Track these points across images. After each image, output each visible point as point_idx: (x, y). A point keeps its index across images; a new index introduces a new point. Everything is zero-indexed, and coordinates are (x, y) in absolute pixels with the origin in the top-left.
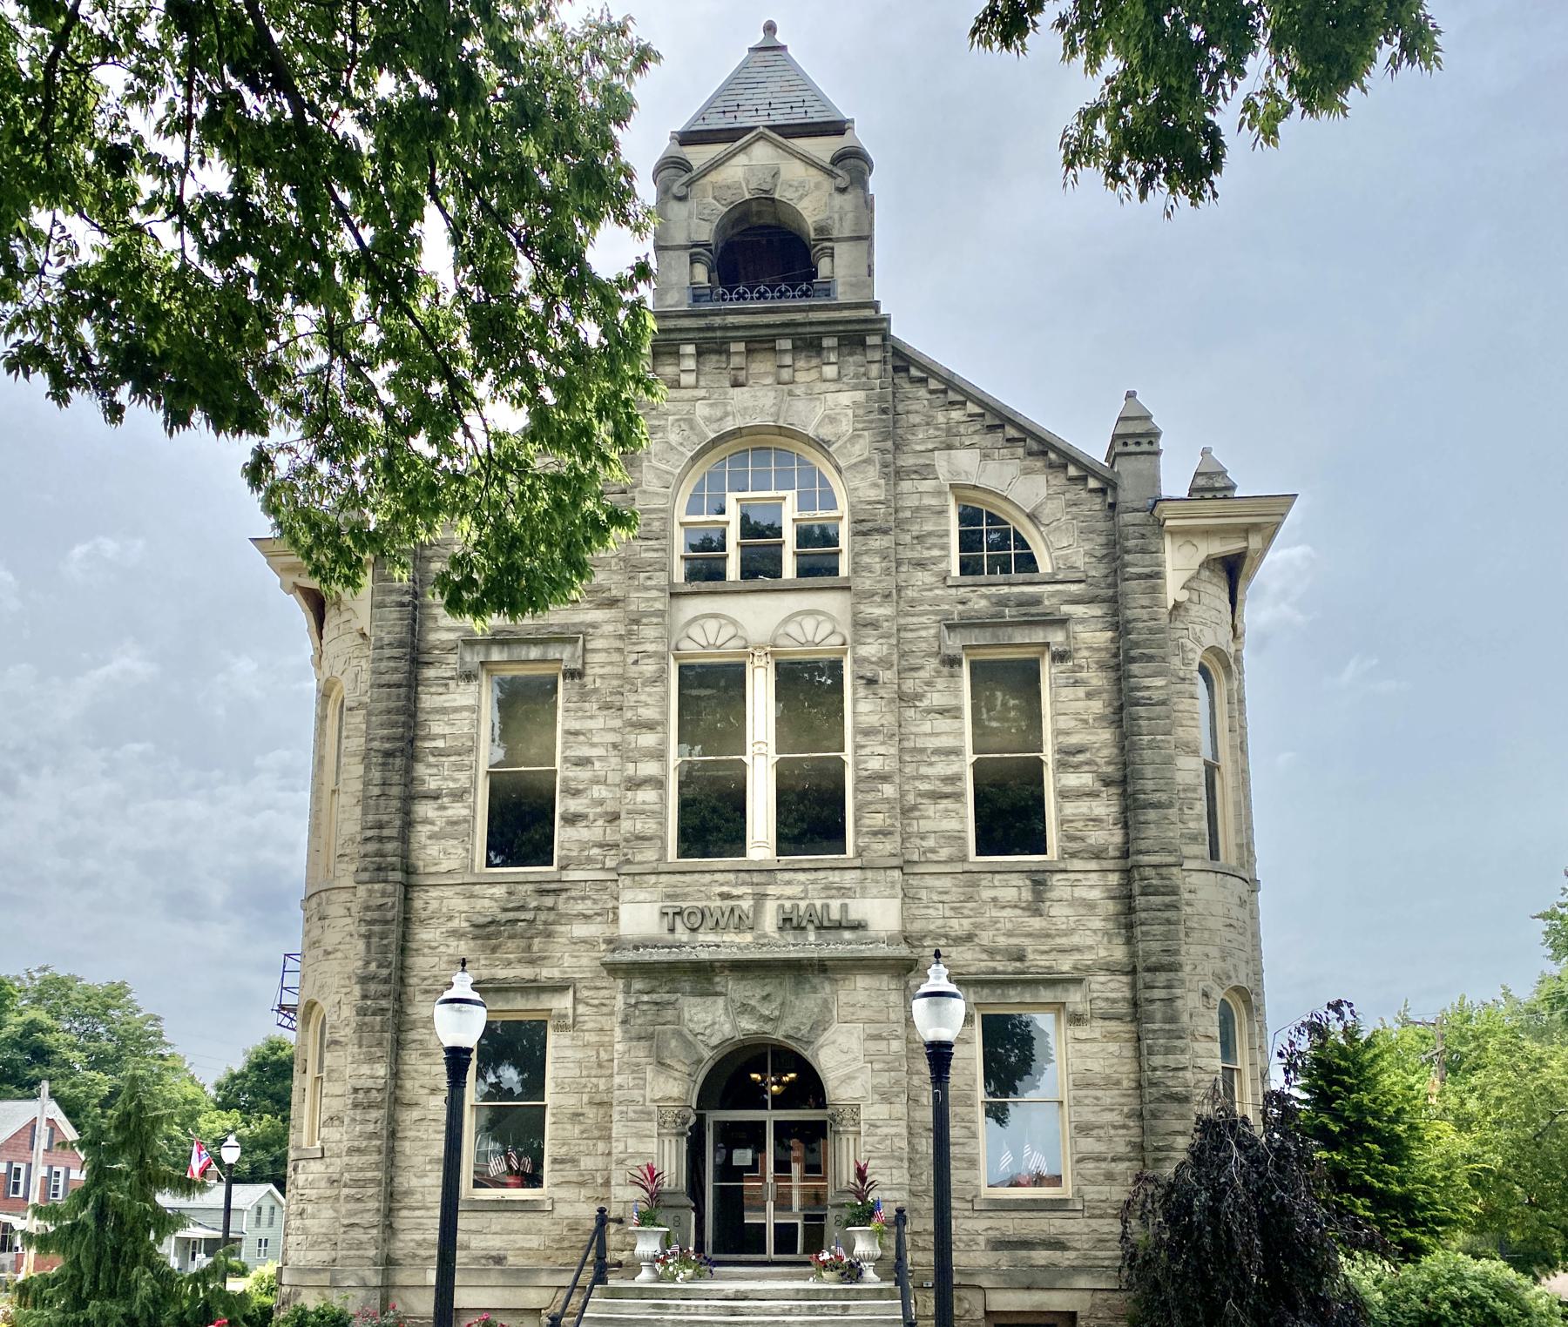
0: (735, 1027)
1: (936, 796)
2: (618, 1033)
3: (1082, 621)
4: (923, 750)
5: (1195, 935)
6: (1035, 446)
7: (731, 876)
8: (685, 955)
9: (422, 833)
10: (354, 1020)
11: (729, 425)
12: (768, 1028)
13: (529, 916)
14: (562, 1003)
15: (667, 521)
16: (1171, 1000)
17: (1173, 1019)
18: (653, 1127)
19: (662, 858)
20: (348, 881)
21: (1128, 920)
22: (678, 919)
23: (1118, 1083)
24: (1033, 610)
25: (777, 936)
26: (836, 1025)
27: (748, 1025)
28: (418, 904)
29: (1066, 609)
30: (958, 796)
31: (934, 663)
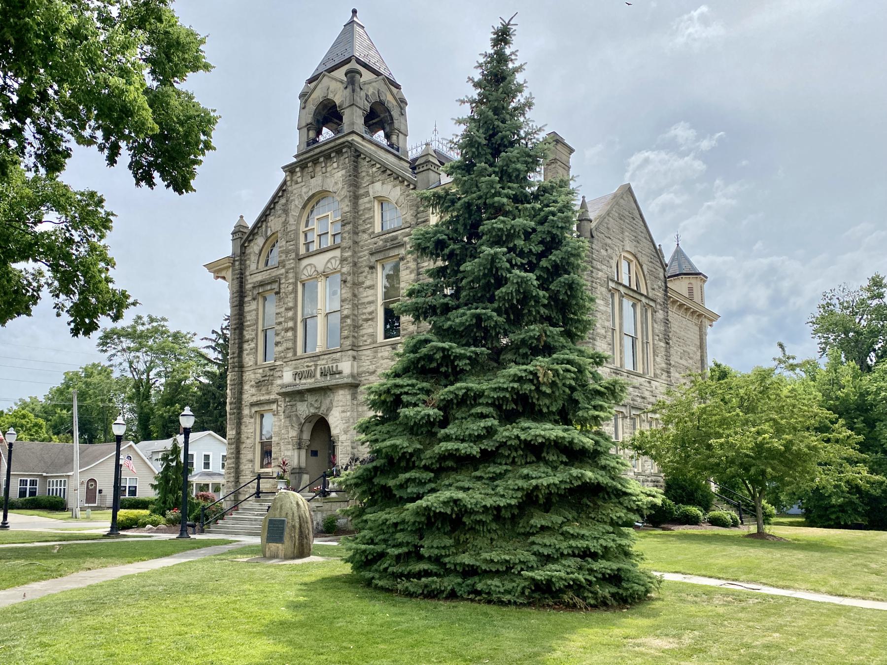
1: (367, 320)
4: (363, 303)
9: (245, 352)
19: (295, 354)
27: (313, 411)
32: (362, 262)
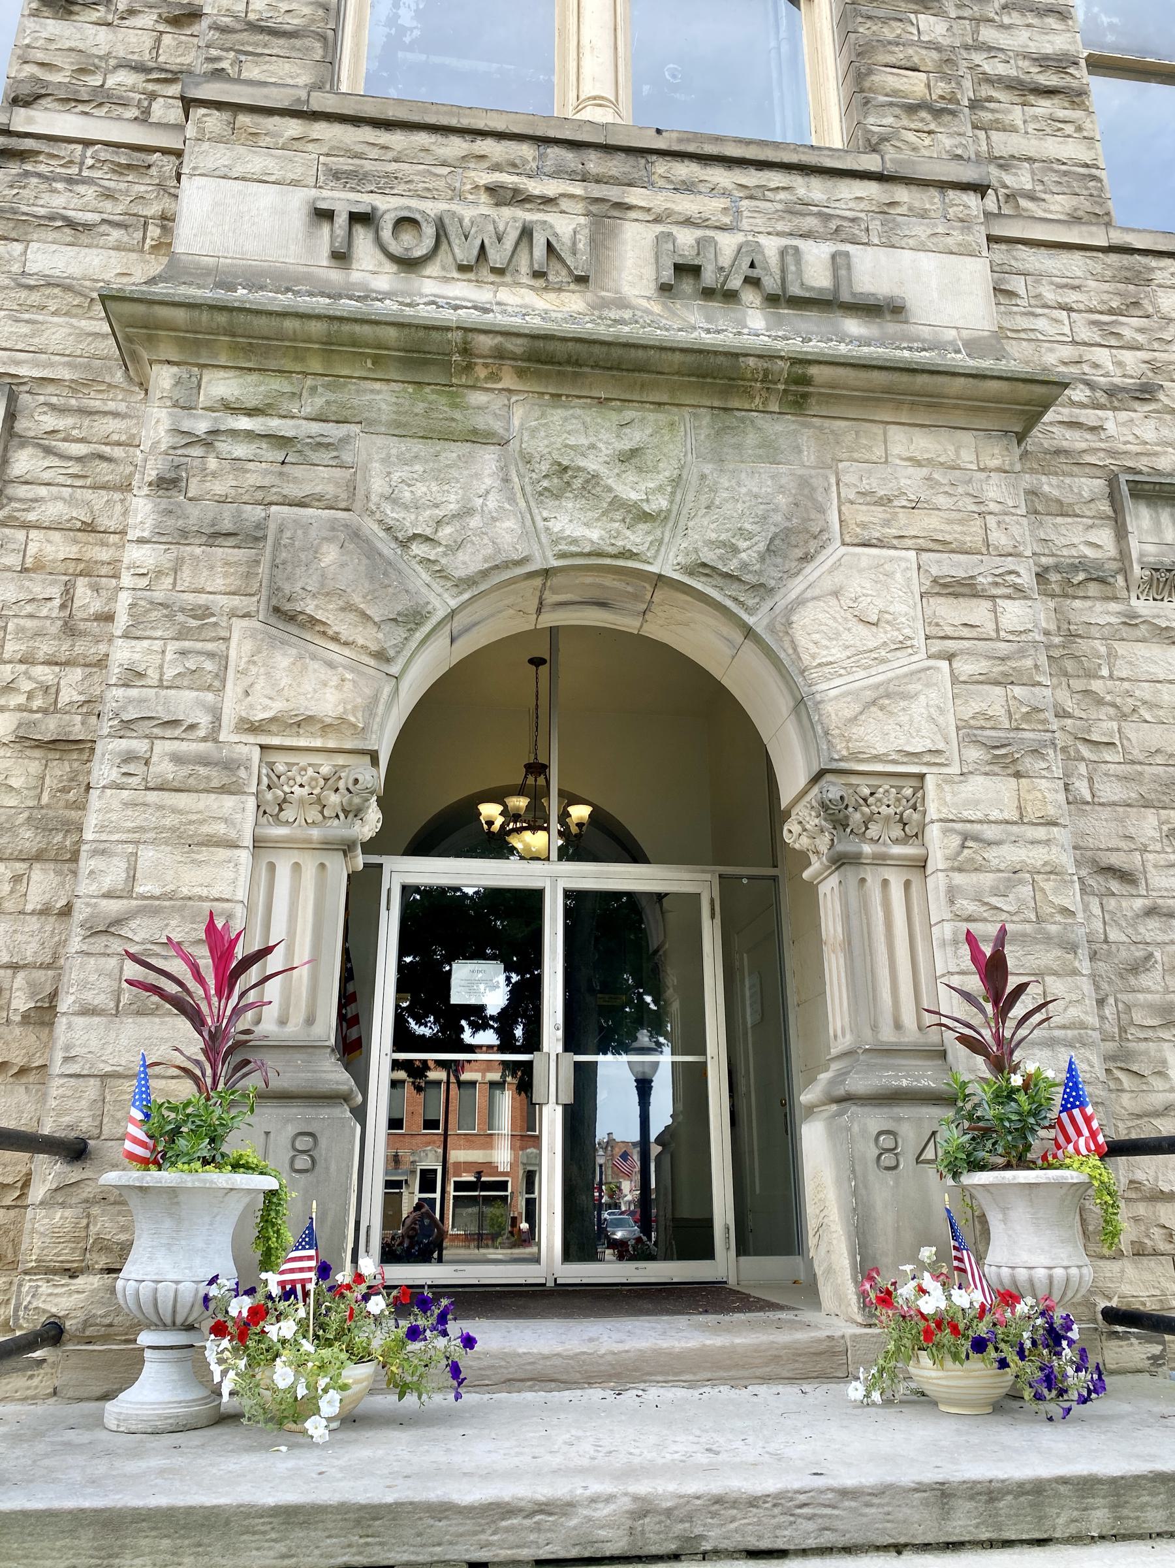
0: (531, 531)
7: (526, 150)
12: (636, 538)
18: (239, 814)
22: (363, 239)
25: (657, 308)
26: (835, 552)
27: (576, 526)
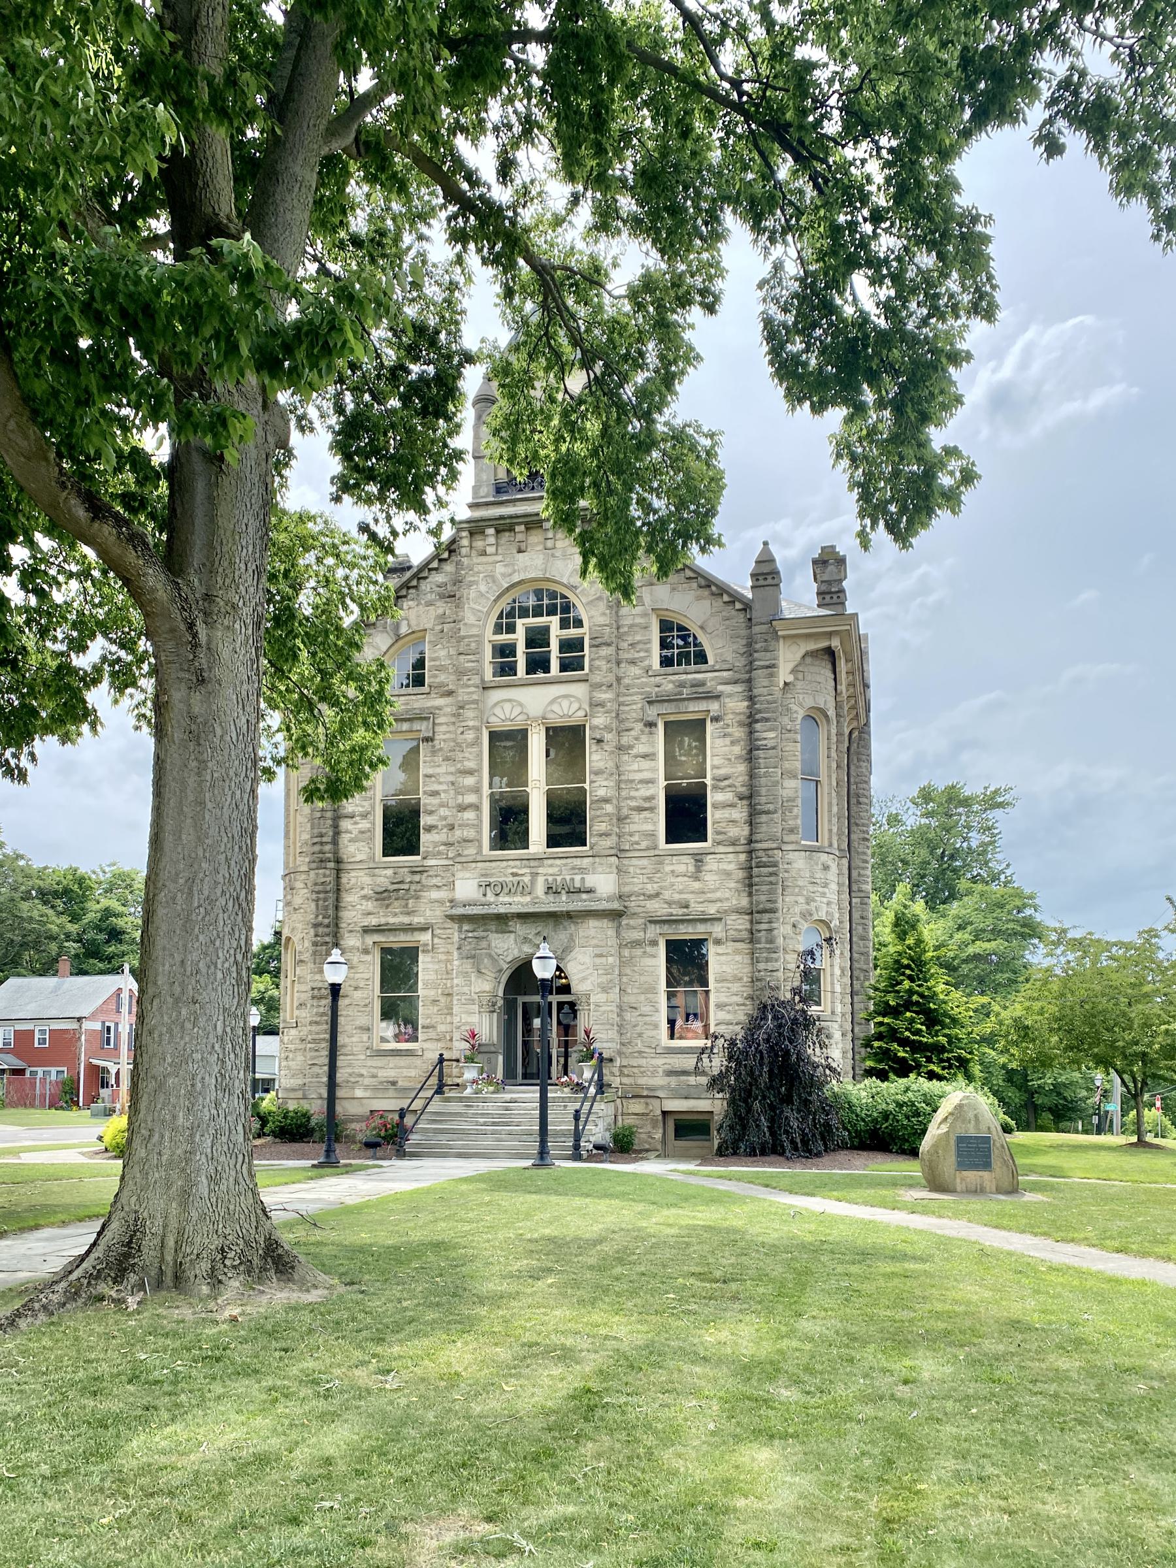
0: (520, 950)
1: (640, 809)
2: (456, 953)
3: (730, 695)
4: (632, 781)
5: (789, 890)
6: (703, 582)
8: (493, 910)
9: (344, 838)
10: (312, 949)
11: (516, 578)
13: (406, 886)
14: (425, 937)
15: (480, 643)
16: (771, 930)
17: (771, 941)
19: (480, 852)
20: (304, 868)
21: (750, 884)
23: (741, 979)
24: (700, 690)
28: (344, 880)
29: (720, 688)
30: (652, 809)
31: (640, 726)
32: (628, 712)
